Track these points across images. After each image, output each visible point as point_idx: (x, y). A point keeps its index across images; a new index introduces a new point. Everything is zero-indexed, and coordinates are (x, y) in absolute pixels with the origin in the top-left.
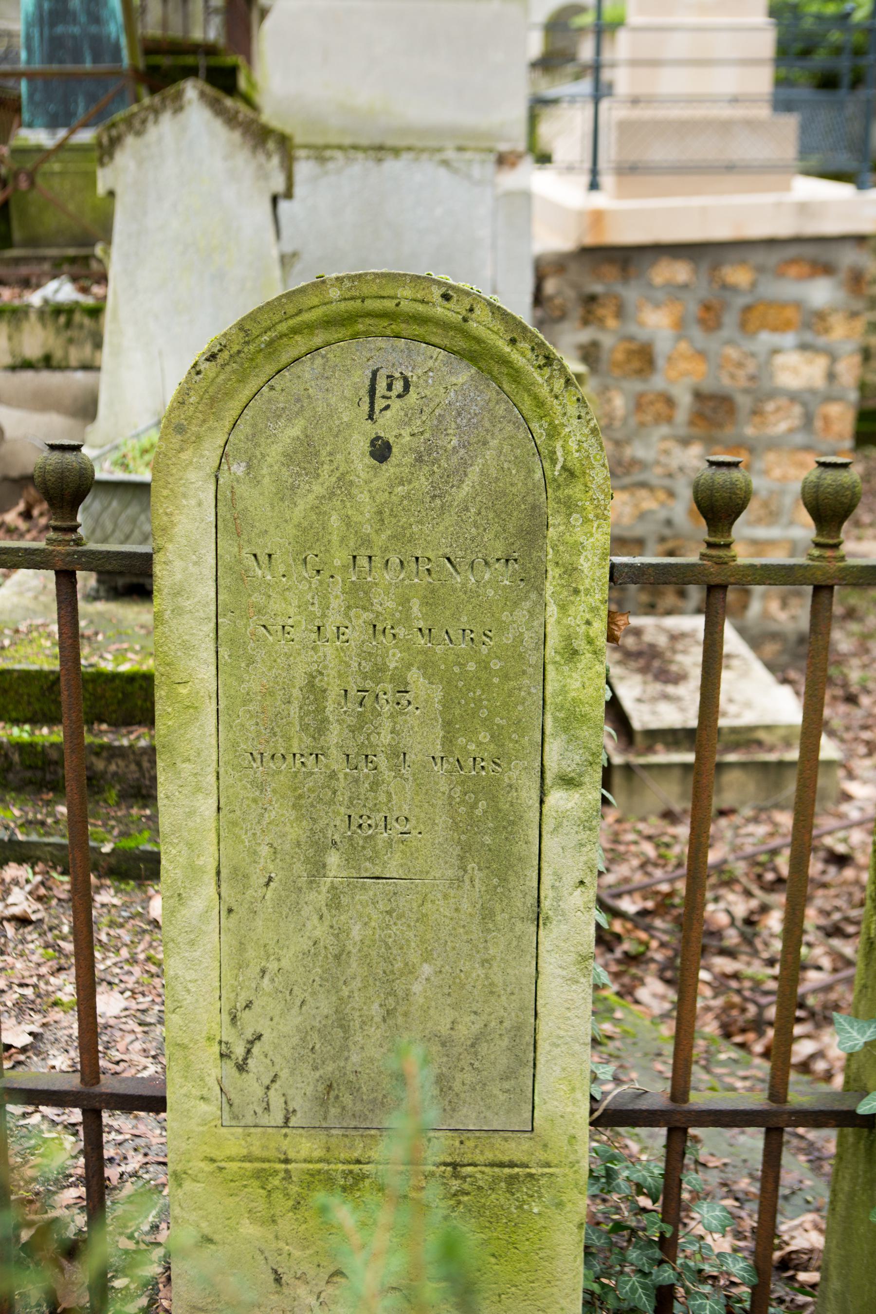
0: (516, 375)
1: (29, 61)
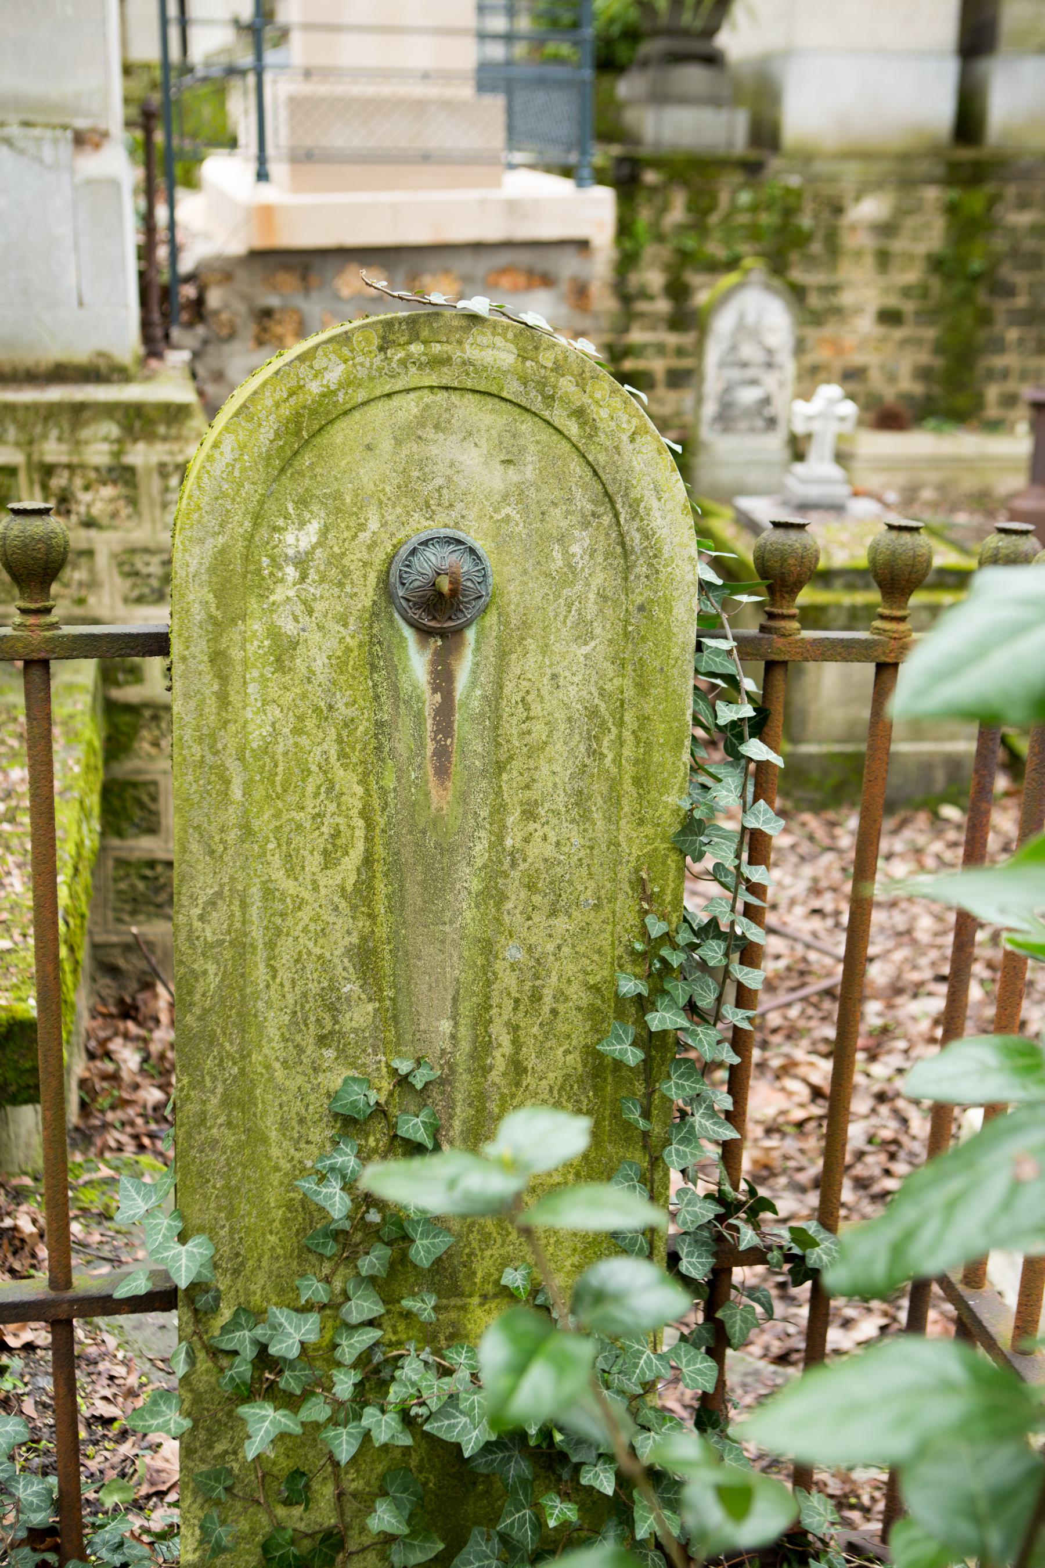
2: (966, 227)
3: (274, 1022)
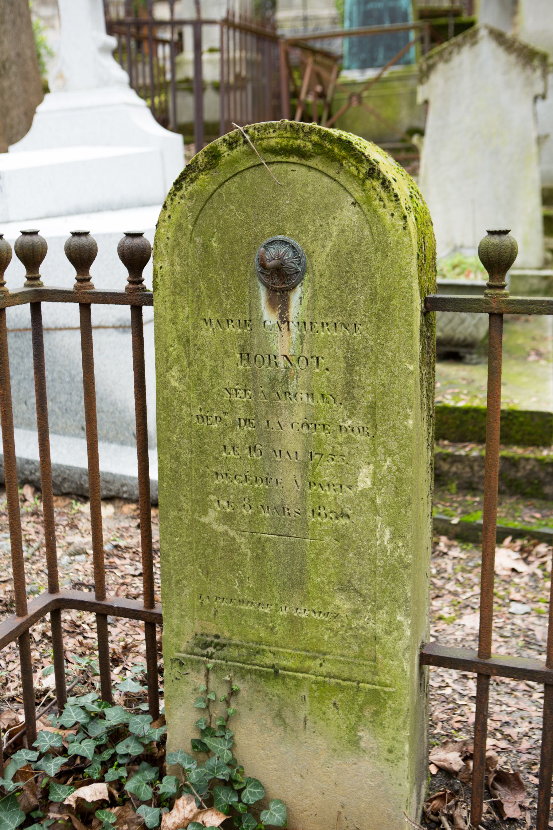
1: (351, 25)
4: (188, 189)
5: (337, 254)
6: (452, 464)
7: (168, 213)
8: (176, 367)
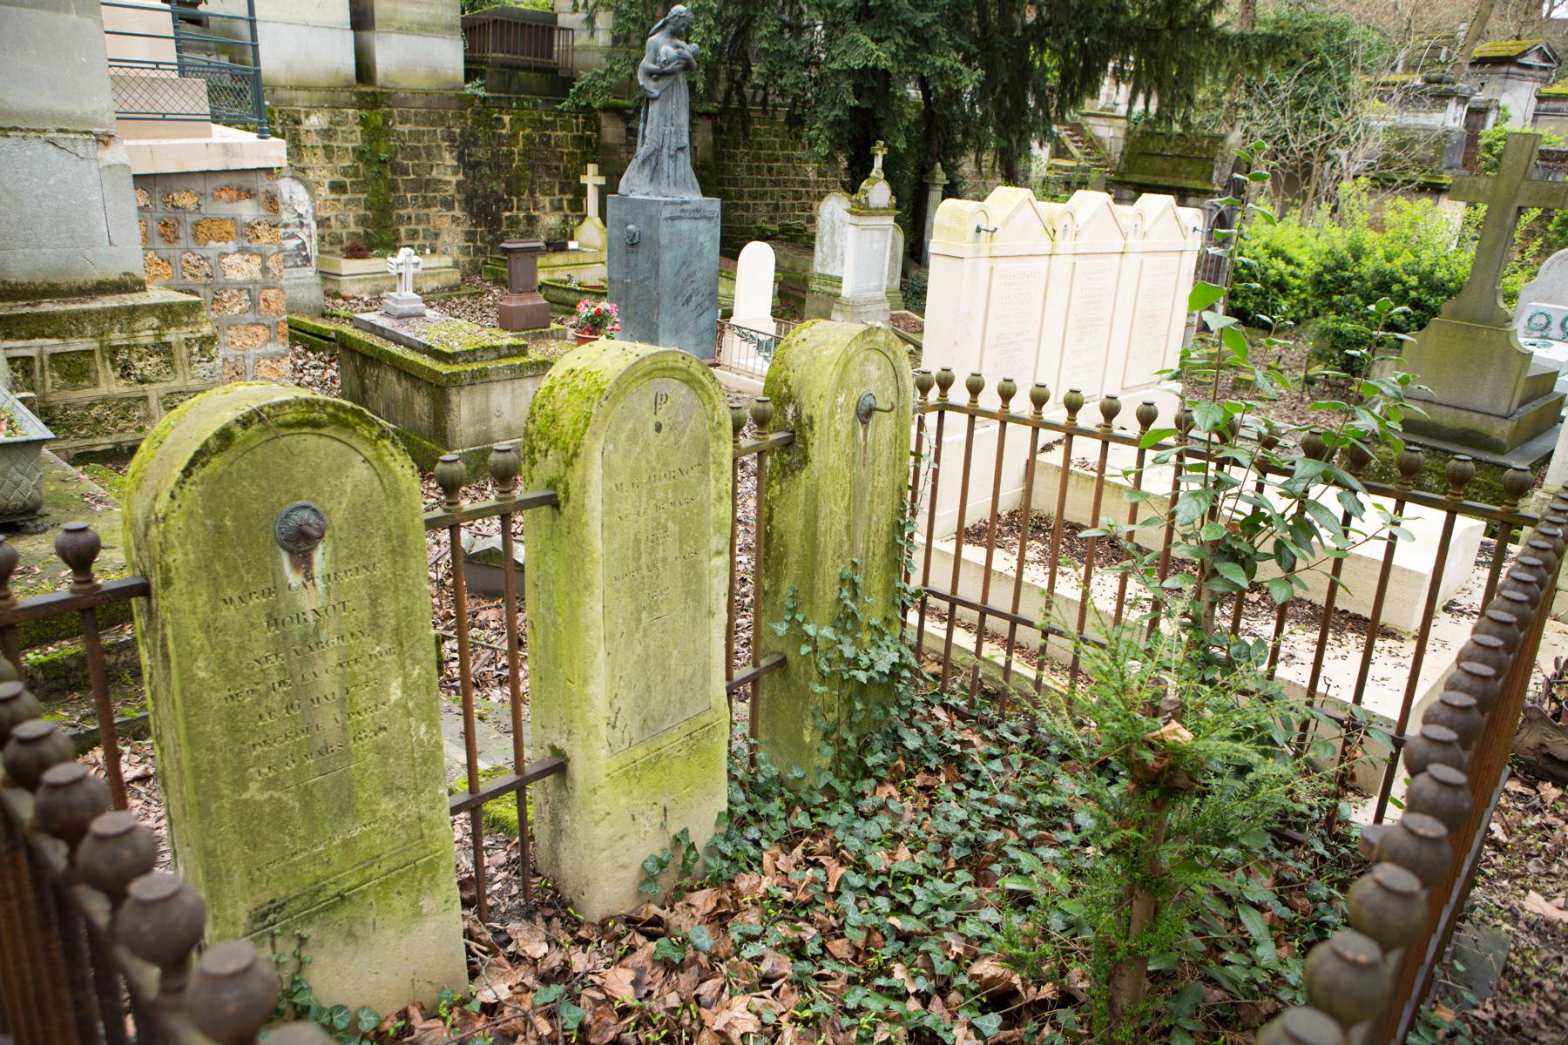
0: (703, 387)
2: (375, 133)
3: (830, 552)
4: (198, 474)
5: (353, 507)
6: (118, 654)
7: (177, 503)
8: (201, 657)
